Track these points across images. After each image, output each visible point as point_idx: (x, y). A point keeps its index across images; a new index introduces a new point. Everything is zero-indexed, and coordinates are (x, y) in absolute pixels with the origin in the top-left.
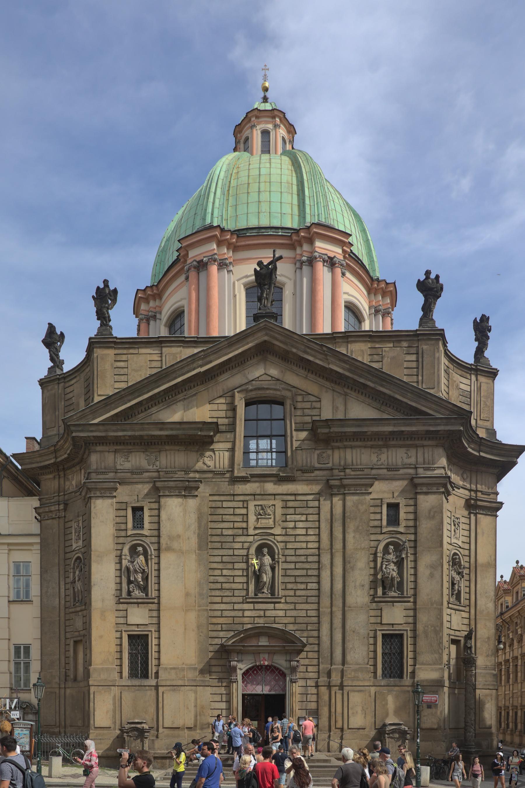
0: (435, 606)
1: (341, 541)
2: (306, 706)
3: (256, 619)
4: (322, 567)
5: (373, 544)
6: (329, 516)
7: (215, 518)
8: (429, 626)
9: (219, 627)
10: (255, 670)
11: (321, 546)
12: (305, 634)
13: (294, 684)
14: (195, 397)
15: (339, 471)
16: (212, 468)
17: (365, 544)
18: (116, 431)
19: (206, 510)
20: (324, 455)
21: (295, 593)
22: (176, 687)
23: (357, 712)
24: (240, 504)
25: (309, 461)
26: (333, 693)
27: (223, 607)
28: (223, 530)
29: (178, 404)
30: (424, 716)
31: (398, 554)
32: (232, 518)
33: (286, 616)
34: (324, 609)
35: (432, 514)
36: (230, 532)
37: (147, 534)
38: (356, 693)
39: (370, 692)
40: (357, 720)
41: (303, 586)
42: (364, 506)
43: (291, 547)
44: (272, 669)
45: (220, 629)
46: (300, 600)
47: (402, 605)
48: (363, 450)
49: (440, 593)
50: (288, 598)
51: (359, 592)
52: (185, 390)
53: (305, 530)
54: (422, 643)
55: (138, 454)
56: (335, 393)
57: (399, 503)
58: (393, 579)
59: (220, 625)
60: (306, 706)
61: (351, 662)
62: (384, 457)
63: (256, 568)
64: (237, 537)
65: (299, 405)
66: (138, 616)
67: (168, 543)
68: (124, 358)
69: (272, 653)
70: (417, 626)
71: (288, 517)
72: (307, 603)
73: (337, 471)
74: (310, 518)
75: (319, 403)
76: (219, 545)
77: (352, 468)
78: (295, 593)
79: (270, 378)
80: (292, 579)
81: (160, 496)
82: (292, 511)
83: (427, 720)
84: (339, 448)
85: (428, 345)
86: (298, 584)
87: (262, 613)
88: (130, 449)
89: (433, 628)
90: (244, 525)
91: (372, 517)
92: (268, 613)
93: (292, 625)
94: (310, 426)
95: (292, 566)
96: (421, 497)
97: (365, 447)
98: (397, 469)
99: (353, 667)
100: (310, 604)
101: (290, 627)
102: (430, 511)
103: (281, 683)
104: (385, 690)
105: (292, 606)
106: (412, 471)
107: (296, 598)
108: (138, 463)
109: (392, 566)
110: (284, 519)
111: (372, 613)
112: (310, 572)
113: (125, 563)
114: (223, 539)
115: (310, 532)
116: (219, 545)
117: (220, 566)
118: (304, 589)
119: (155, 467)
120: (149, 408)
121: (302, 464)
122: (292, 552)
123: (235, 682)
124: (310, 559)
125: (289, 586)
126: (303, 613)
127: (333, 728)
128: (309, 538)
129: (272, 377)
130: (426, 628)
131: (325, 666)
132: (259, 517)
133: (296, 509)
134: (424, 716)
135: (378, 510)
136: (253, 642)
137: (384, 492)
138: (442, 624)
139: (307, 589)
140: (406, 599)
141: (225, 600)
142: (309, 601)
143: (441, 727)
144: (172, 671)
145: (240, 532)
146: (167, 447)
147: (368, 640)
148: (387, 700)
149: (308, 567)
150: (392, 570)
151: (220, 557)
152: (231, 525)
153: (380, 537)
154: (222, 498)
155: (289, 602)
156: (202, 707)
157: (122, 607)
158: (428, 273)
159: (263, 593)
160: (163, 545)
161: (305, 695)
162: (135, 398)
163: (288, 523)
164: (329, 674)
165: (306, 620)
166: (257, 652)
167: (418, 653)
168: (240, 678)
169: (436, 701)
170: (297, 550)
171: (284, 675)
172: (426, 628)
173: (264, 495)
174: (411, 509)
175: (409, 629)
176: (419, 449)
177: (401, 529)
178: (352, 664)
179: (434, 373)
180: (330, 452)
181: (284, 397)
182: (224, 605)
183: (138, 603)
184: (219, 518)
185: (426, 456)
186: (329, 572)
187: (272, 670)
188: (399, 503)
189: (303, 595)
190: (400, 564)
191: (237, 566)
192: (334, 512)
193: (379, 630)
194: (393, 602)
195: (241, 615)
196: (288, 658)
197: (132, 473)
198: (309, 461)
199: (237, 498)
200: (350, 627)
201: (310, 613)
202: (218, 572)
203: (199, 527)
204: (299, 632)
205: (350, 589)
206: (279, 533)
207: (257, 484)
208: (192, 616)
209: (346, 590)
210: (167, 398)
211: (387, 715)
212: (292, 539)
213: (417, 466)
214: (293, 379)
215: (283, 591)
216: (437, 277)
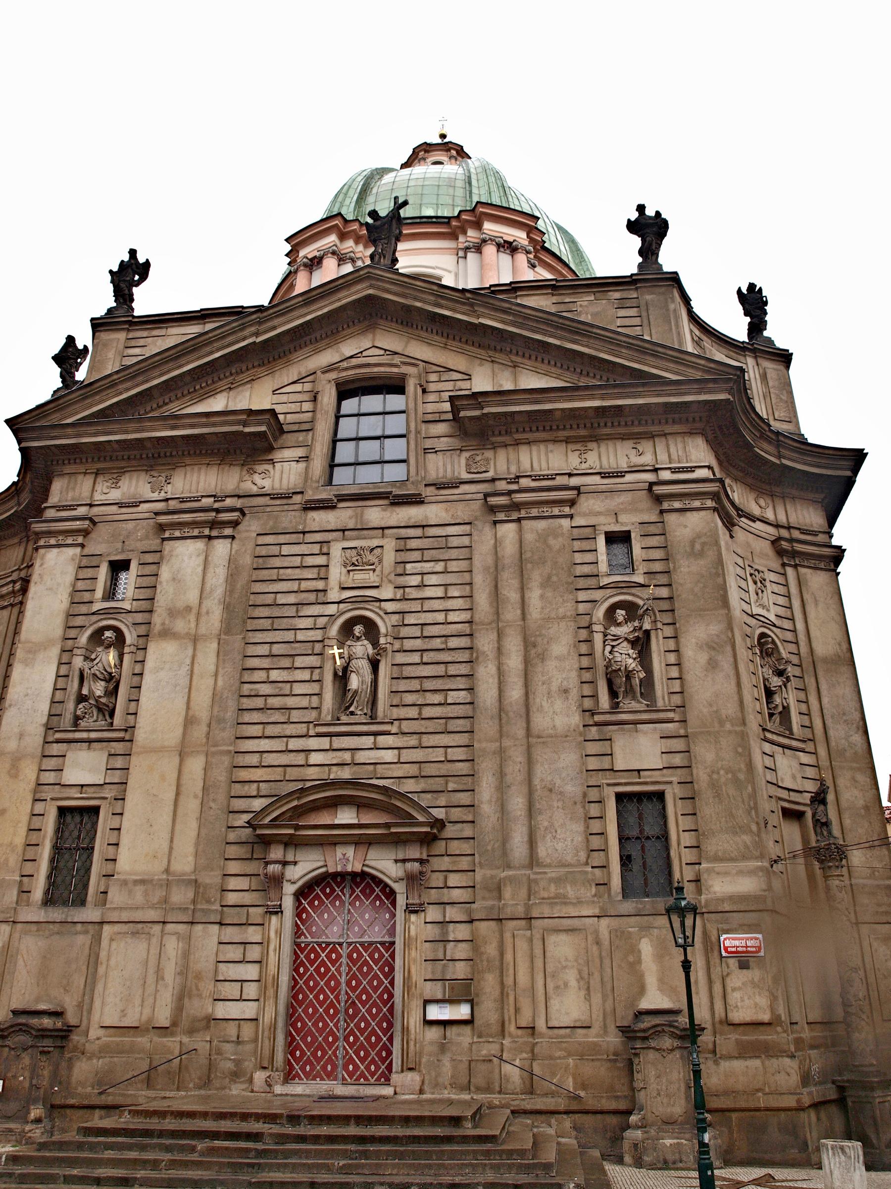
0: (728, 726)
1: (518, 606)
2: (443, 972)
3: (334, 768)
4: (477, 658)
5: (582, 608)
6: (490, 560)
7: (264, 575)
8: (722, 772)
9: (252, 789)
10: (328, 885)
11: (477, 618)
12: (442, 800)
13: (413, 917)
14: (249, 386)
15: (508, 483)
16: (268, 490)
17: (568, 608)
18: (96, 434)
20: (478, 458)
21: (420, 713)
22: (140, 926)
23: (566, 985)
24: (316, 549)
25: (449, 470)
26: (508, 936)
27: (265, 745)
28: (279, 595)
29: (219, 396)
31: (636, 624)
32: (297, 574)
33: (399, 762)
34: (484, 745)
35: (698, 547)
36: (292, 599)
37: (128, 607)
38: (563, 937)
39: (596, 932)
40: (569, 1007)
41: (437, 698)
42: (560, 539)
43: (412, 621)
44: (365, 882)
45: (255, 793)
46: (431, 726)
47: (655, 729)
48: (551, 446)
49: (736, 698)
50: (404, 723)
51: (559, 704)
52: (231, 374)
53: (442, 588)
54: (709, 809)
55: (135, 474)
56: (496, 365)
57: (629, 532)
58: (629, 675)
59: (256, 785)
60: (443, 972)
61: (549, 861)
63: (338, 663)
64: (305, 607)
65: (432, 387)
67: (167, 622)
68: (141, 342)
69: (364, 842)
70: (695, 771)
71: (408, 566)
73: (504, 482)
74: (453, 566)
75: (469, 382)
76: (266, 624)
77: (530, 476)
78: (420, 713)
79: (382, 352)
80: (415, 685)
81: (164, 540)
82: (416, 555)
85: (653, 294)
86: (428, 694)
87: (347, 757)
88: (123, 468)
89: (730, 776)
90: (320, 585)
91: (578, 557)
92: (361, 757)
93: (412, 780)
94: (450, 416)
95: (416, 658)
96: (672, 519)
97: (555, 441)
98: (620, 474)
99: (552, 873)
100: (452, 735)
101: (409, 786)
102: (692, 543)
103: (387, 916)
104: (632, 925)
105: (413, 741)
106: (650, 477)
107: (423, 722)
108: (133, 489)
109: (625, 648)
110: (400, 570)
111: (592, 748)
112: (453, 670)
113: (78, 662)
114: (276, 612)
115: (454, 592)
116: (266, 624)
117: (265, 663)
118: (440, 704)
119: (163, 494)
120: (167, 404)
121: (437, 475)
122: (416, 632)
123: (276, 913)
124: (453, 643)
125: (409, 699)
126: (438, 754)
127: (512, 1028)
128: (450, 604)
129: (386, 350)
130: (715, 776)
131: (489, 873)
132: (351, 568)
133: (425, 552)
135: (586, 545)
136: (324, 818)
137: (599, 513)
138: (750, 766)
139: (444, 704)
140: (662, 715)
141: (270, 730)
143: (779, 1016)
144: (137, 888)
145: (312, 597)
146: (188, 462)
147: (584, 807)
148: (640, 951)
149: (450, 659)
150: (626, 657)
151: (267, 646)
152: (294, 586)
153: (597, 595)
154: (282, 539)
155: (407, 731)
156: (198, 976)
157: (56, 749)
158: (641, 208)
159: (352, 713)
160: (157, 627)
161: (441, 944)
162: (137, 385)
163: (408, 577)
164: (497, 889)
165: (445, 769)
166: (328, 842)
167: (704, 834)
168: (288, 903)
170: (425, 627)
171: (391, 895)
172: (715, 776)
173: (363, 529)
175: (675, 779)
176: (656, 439)
177: (639, 578)
178: (549, 866)
179: (671, 329)
180: (489, 454)
181: (403, 378)
182: (267, 741)
183: (90, 741)
184: (273, 574)
185: (673, 450)
186: (492, 668)
187: (368, 884)
188: (629, 532)
189: (438, 715)
190: (641, 644)
191: (299, 662)
192: (499, 555)
193: (608, 785)
195: (302, 762)
196: (401, 856)
197: (121, 505)
198: (449, 470)
199: (309, 538)
200: (542, 780)
201: (453, 754)
202: (260, 676)
203: (232, 592)
204: (429, 796)
205: (539, 698)
206: (389, 596)
207: (350, 512)
208: (195, 765)
209: (531, 700)
210: (198, 387)
211: (642, 990)
213: (657, 466)
214: (420, 351)
215: (395, 710)
216: (658, 214)
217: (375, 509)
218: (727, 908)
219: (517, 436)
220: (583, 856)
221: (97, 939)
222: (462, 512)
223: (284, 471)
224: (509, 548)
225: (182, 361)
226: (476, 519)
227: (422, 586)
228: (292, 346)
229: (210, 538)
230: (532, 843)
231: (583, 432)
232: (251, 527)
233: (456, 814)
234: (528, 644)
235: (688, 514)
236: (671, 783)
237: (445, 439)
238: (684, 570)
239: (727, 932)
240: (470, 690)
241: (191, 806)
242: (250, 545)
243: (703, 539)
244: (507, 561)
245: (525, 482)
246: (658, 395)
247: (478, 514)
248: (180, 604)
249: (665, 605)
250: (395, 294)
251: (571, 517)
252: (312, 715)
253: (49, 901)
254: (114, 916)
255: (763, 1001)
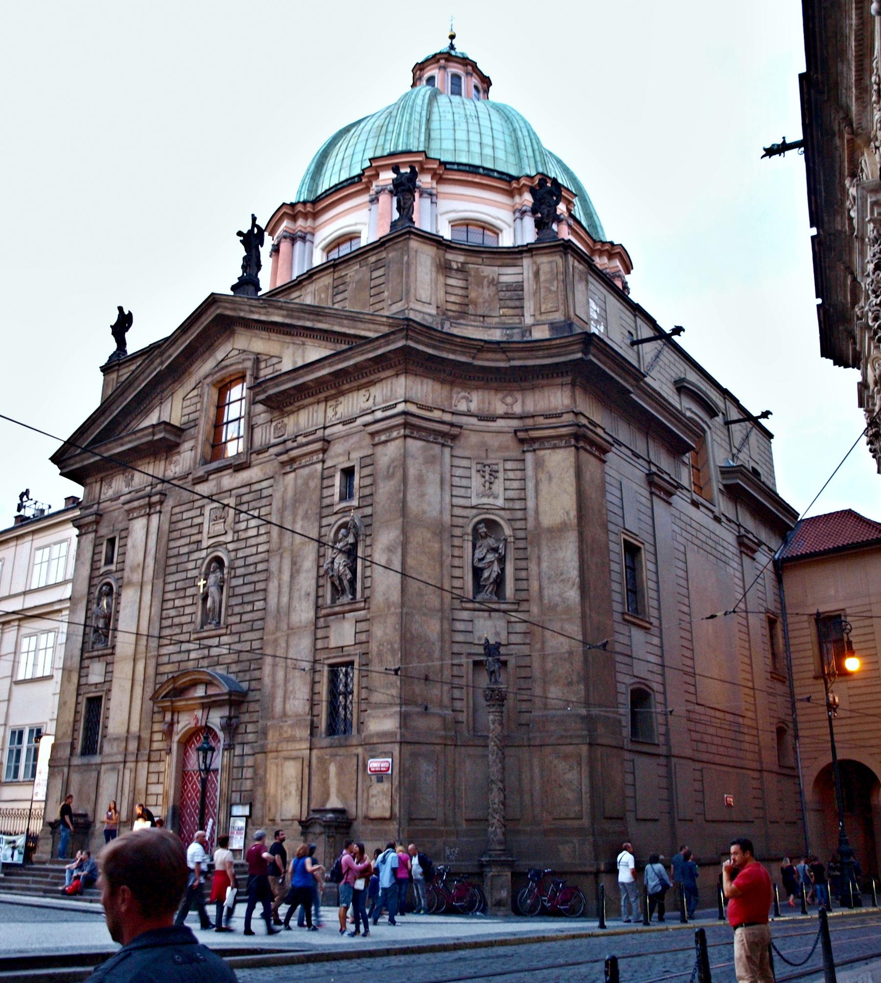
0: (392, 609)
6: (280, 504)
13: (226, 753)
19: (166, 527)
30: (373, 796)
35: (391, 470)
41: (249, 608)
42: (315, 480)
48: (316, 407)
55: (118, 477)
62: (340, 409)
66: (96, 674)
72: (252, 630)
80: (239, 600)
83: (376, 803)
84: (293, 412)
89: (389, 646)
96: (380, 448)
97: (318, 403)
102: (389, 467)
110: (237, 520)
118: (251, 612)
125: (237, 609)
134: (373, 796)
139: (253, 611)
140: (357, 606)
142: (255, 627)
145: (194, 547)
149: (257, 579)
153: (332, 520)
154: (184, 508)
160: (126, 580)
169: (388, 768)
171: (216, 737)
174: (367, 471)
183: (99, 656)
190: (351, 553)
194: (344, 613)
208: (140, 666)
211: (326, 796)
212: (242, 544)
217: (227, 477)
218: (375, 740)
219: (297, 404)
220: (307, 708)
221: (99, 773)
222: (270, 469)
223: (185, 459)
224: (290, 494)
225: (126, 395)
226: (276, 473)
227: (247, 529)
228: (188, 363)
229: (149, 515)
230: (285, 700)
231: (333, 392)
232: (169, 503)
233: (254, 684)
234: (294, 563)
235: (389, 444)
236: (356, 655)
237: (262, 415)
238: (381, 491)
239: (373, 757)
240: (265, 599)
241: (138, 690)
242: (168, 515)
243: (395, 463)
244: (288, 503)
245: (301, 440)
246: (362, 354)
247: (277, 469)
248: (135, 563)
249: (368, 521)
250: (231, 309)
251: (323, 461)
252: (191, 628)
253: (84, 753)
254: (106, 760)
255: (387, 804)
